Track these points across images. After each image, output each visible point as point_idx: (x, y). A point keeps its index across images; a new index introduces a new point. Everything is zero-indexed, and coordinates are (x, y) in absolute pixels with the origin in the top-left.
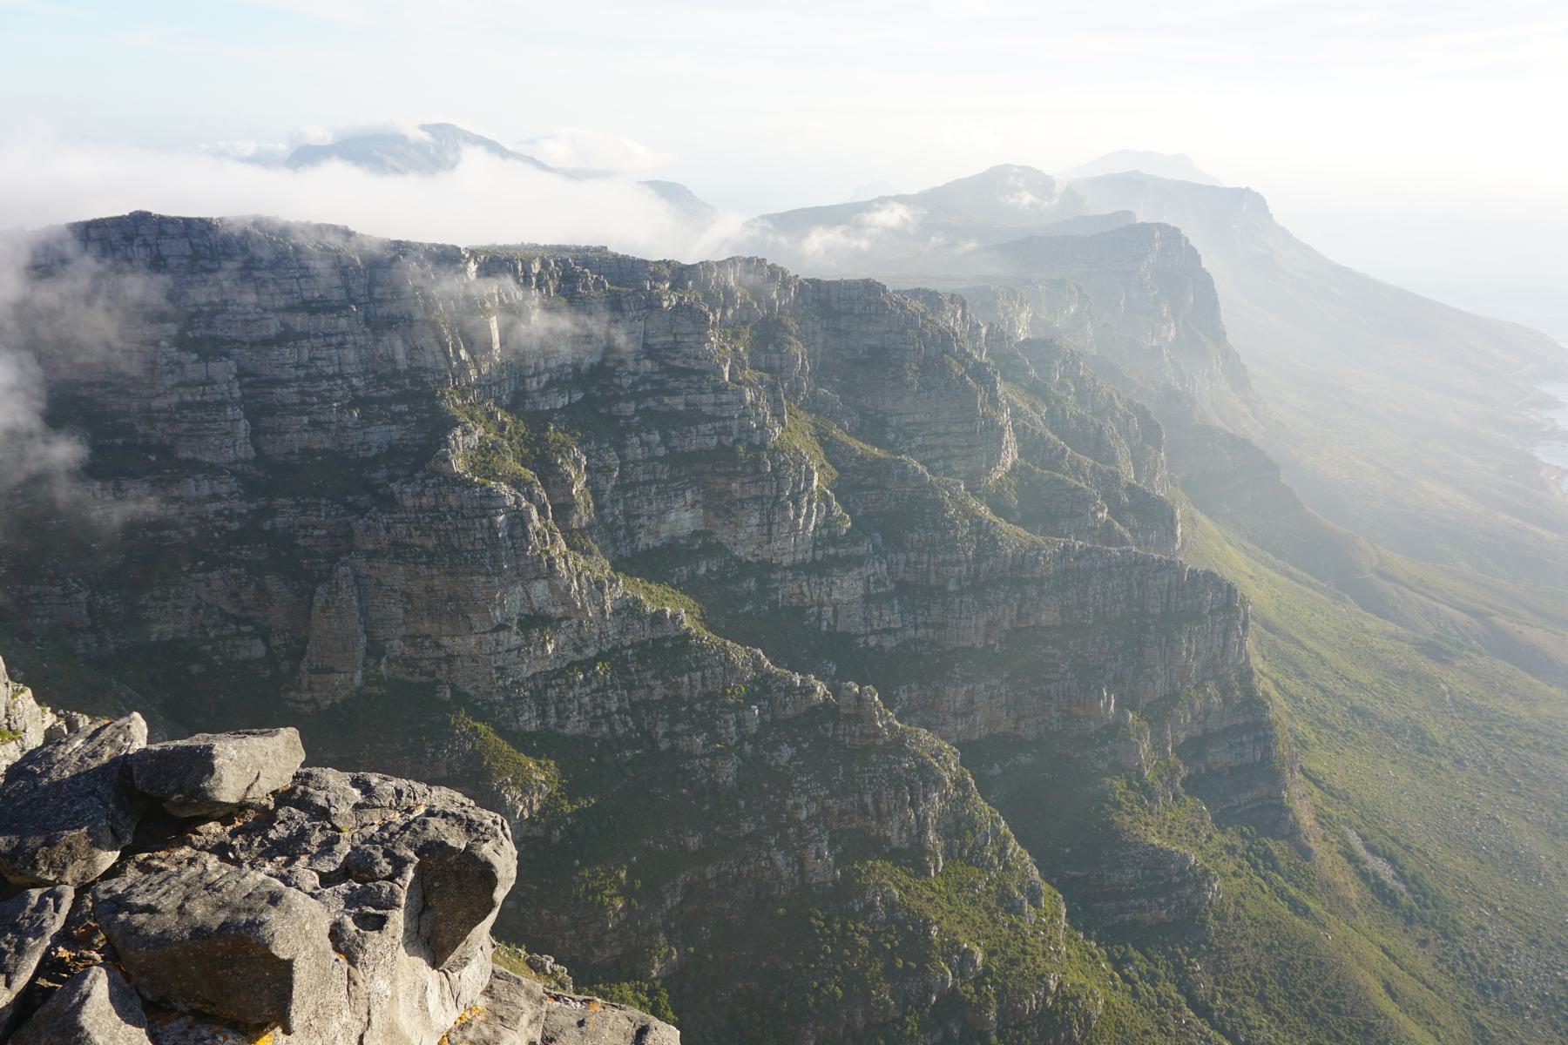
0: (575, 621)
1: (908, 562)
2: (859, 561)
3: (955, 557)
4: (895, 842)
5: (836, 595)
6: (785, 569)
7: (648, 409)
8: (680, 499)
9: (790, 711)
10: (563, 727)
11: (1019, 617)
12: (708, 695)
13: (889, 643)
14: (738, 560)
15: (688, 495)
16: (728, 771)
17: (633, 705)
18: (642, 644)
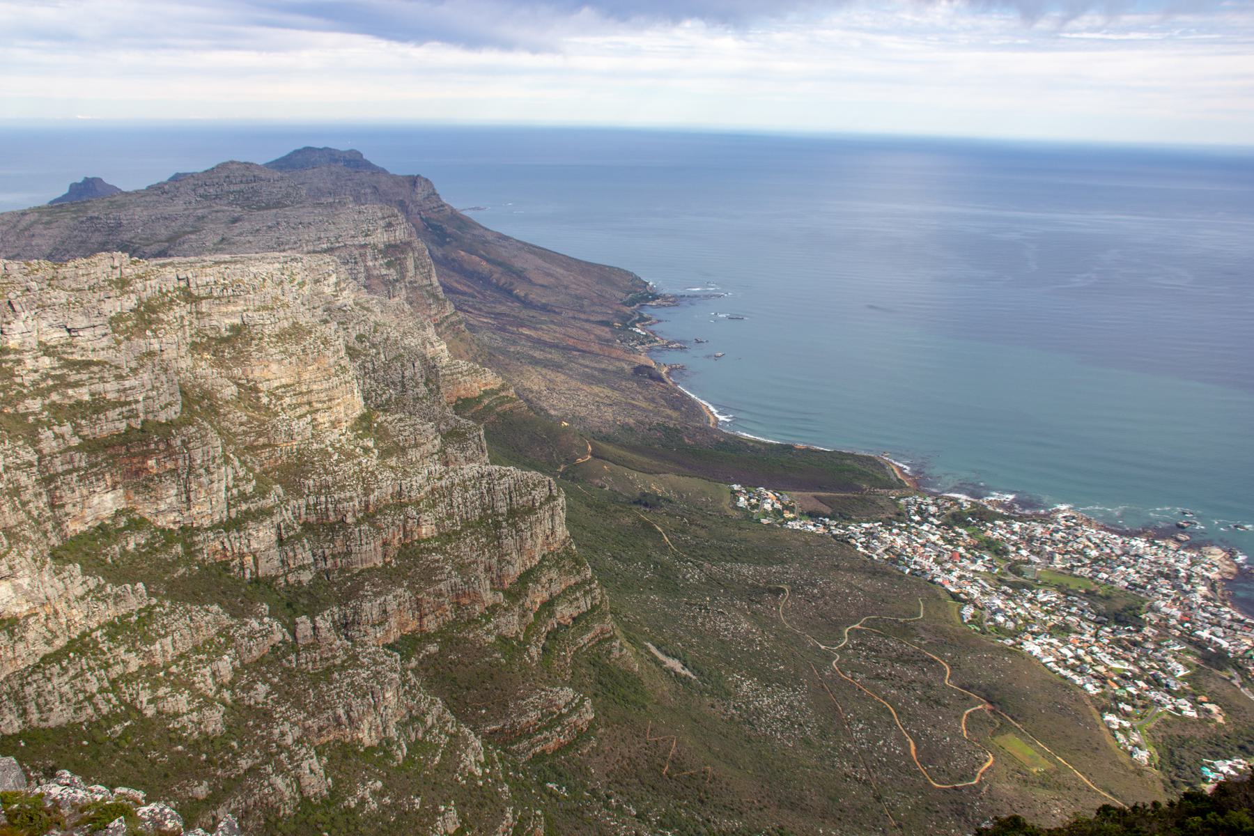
0: (43, 615)
1: (307, 506)
2: (269, 512)
3: (348, 494)
4: (367, 742)
5: (254, 545)
6: (206, 530)
7: (53, 404)
8: (102, 483)
9: (256, 653)
10: (46, 720)
11: (405, 536)
12: (182, 656)
13: (306, 577)
14: (163, 530)
15: (107, 476)
16: (215, 721)
17: (113, 682)
18: (112, 624)
